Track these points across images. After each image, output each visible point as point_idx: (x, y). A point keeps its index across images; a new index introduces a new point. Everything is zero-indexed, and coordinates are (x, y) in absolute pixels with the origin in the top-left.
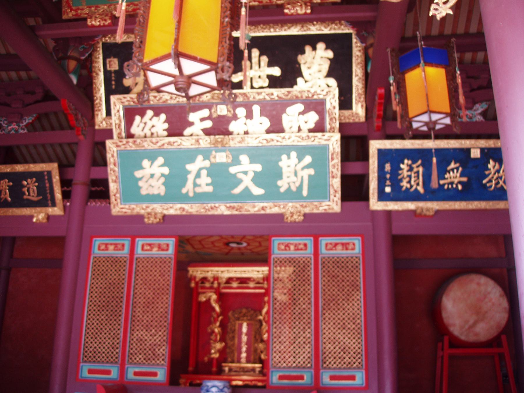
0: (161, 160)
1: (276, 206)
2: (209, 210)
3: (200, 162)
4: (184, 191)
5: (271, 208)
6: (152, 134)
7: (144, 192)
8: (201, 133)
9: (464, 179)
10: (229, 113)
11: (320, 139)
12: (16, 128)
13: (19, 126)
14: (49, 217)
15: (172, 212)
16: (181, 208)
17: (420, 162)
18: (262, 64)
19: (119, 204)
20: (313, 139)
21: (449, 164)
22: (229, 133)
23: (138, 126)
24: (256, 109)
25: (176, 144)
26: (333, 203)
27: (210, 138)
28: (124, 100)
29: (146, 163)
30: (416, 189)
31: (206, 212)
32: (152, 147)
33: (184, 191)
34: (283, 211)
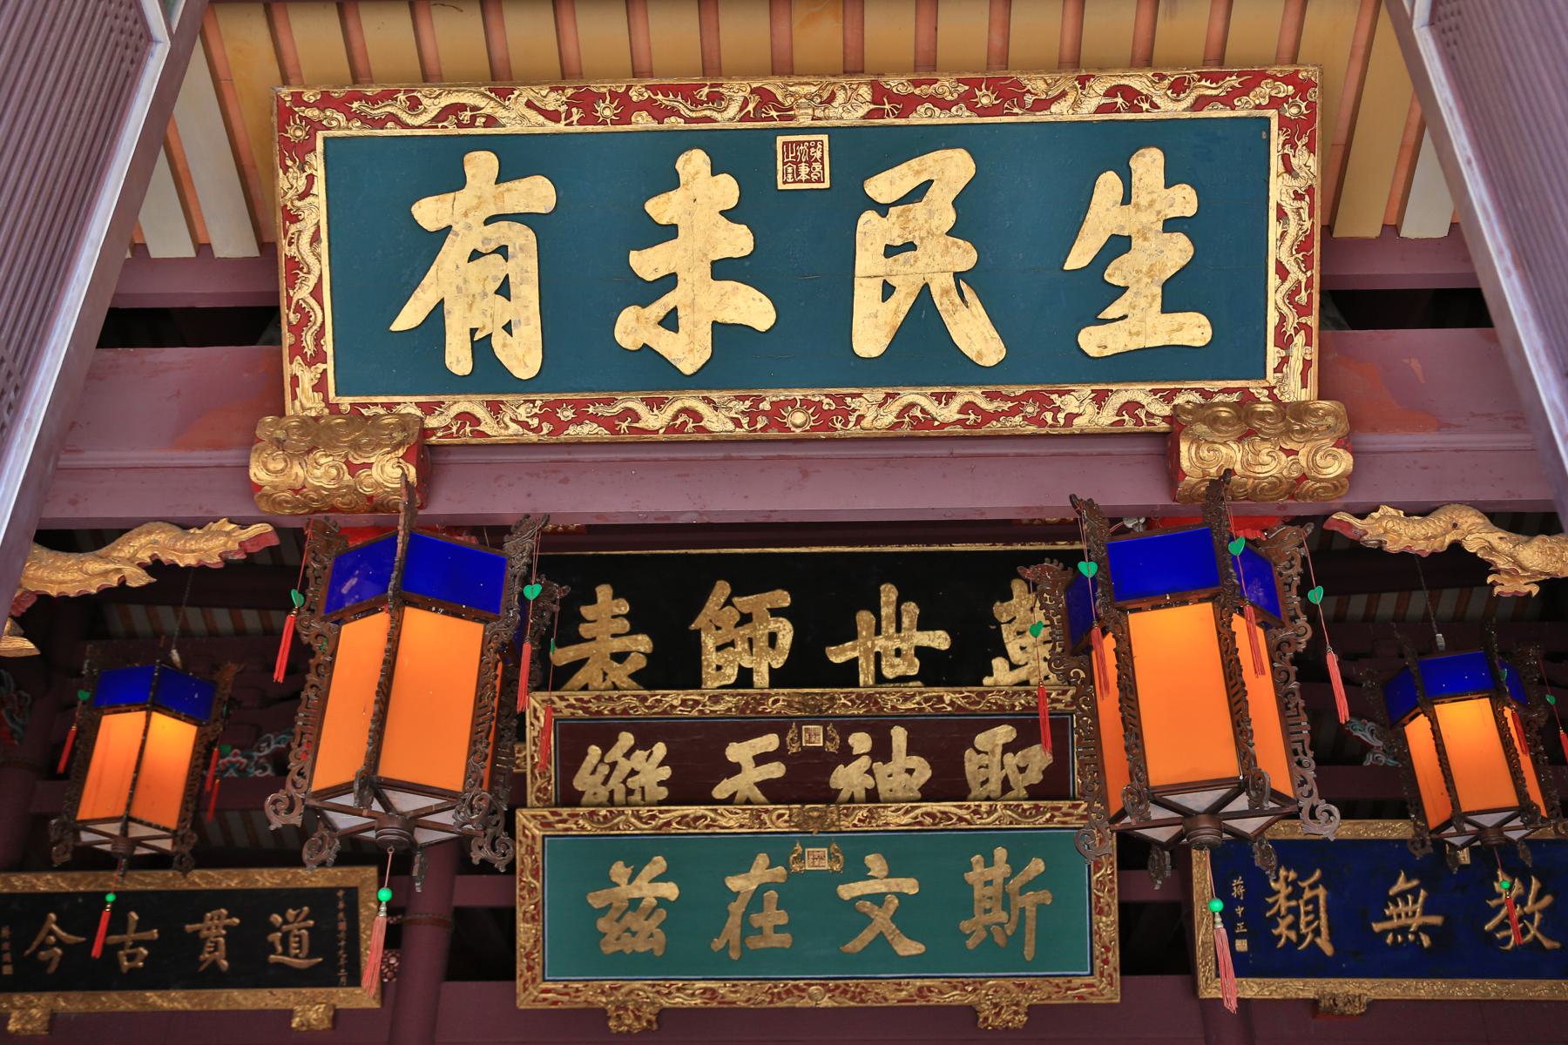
0: (659, 864)
1: (955, 988)
2: (781, 999)
3: (761, 871)
4: (718, 944)
5: (941, 993)
6: (630, 792)
7: (609, 948)
8: (758, 794)
9: (1436, 920)
10: (828, 743)
11: (1066, 815)
12: (242, 763)
13: (249, 758)
14: (337, 1016)
15: (679, 1000)
16: (705, 990)
17: (1318, 874)
18: (906, 621)
19: (539, 980)
20: (1048, 815)
21: (1394, 882)
22: (831, 796)
23: (594, 772)
24: (899, 736)
25: (701, 823)
26: (1102, 982)
27: (790, 809)
28: (560, 704)
29: (619, 871)
30: (1313, 943)
31: (771, 1002)
32: (637, 829)
33: (718, 944)
34: (972, 998)
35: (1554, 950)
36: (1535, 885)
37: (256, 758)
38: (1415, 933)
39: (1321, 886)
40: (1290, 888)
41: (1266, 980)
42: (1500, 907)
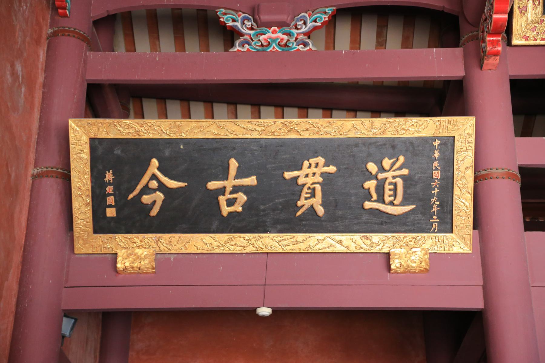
12: (282, 39)
13: (289, 34)
37: (296, 35)
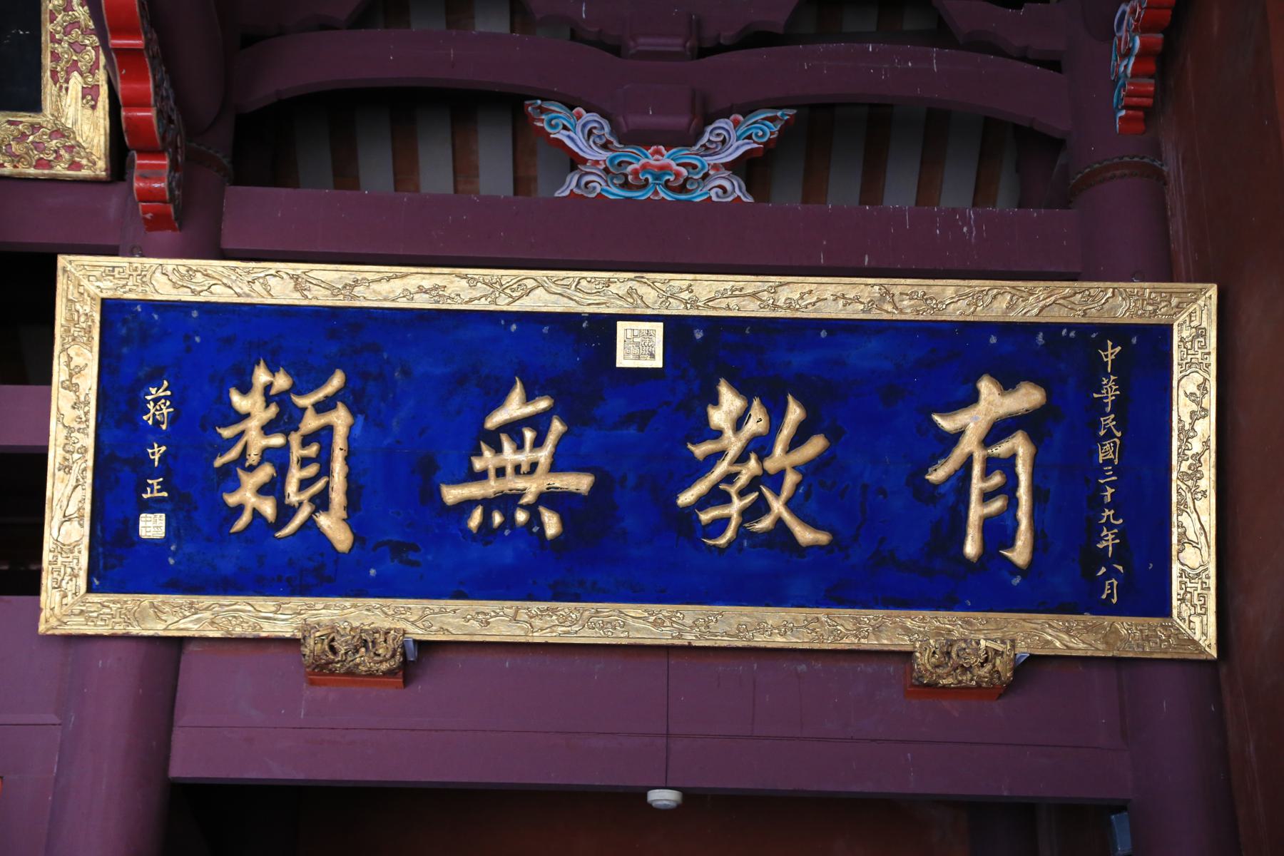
9: (579, 483)
17: (337, 381)
21: (499, 400)
35: (814, 548)
36: (795, 413)
38: (532, 509)
39: (340, 405)
40: (273, 410)
41: (195, 598)
42: (719, 455)
